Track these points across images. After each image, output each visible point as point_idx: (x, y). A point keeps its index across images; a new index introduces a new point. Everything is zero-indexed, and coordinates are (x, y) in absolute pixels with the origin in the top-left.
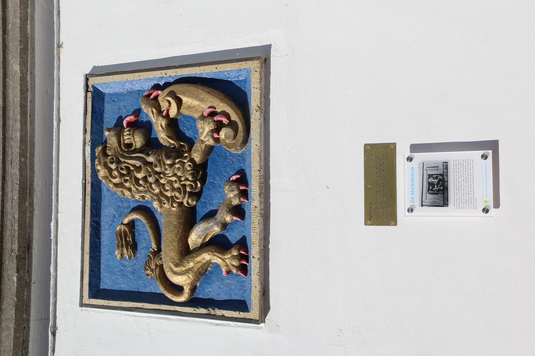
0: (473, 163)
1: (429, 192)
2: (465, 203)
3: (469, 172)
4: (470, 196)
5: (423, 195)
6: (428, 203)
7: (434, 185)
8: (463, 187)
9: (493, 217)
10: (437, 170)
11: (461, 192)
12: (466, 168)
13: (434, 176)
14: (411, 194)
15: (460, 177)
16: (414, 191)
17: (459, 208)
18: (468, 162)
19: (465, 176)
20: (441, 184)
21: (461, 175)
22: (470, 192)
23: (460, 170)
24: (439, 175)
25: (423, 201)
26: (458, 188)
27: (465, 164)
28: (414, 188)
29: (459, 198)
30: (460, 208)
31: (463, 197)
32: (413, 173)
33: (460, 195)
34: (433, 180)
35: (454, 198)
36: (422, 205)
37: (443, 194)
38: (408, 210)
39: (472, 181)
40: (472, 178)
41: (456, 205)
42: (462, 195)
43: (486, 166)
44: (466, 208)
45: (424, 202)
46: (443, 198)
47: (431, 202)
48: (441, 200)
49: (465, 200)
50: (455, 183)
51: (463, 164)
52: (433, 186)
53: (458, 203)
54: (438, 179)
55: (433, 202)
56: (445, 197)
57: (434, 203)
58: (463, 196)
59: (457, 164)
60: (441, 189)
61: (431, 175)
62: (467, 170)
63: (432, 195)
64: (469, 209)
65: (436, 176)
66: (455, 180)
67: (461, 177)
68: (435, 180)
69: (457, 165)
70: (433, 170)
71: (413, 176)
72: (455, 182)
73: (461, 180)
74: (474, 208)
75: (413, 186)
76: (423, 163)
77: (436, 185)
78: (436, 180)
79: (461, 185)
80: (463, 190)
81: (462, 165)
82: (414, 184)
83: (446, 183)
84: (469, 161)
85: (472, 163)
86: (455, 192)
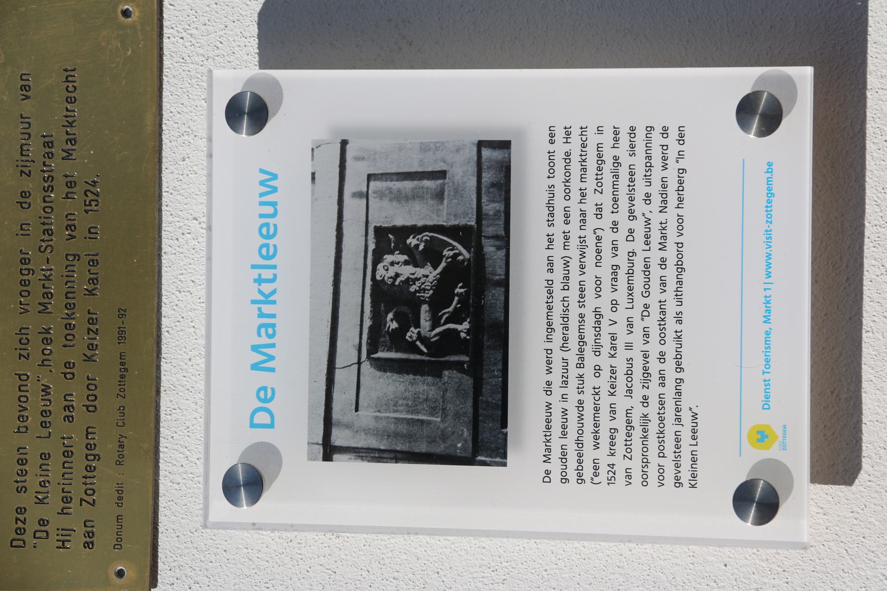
0: (680, 155)
1: (381, 355)
2: (621, 437)
3: (656, 219)
4: (654, 390)
5: (339, 375)
6: (367, 431)
7: (415, 303)
8: (613, 329)
9: (805, 547)
10: (439, 195)
12: (632, 188)
13: (412, 241)
14: (255, 367)
15: (591, 253)
16: (273, 346)
17: (580, 480)
18: (648, 148)
19: (624, 247)
20: (463, 299)
21: (599, 239)
22: (654, 367)
23: (592, 199)
24: (453, 231)
25: (336, 415)
26: (573, 334)
27: (625, 160)
28: (273, 326)
29: (581, 402)
30: (588, 473)
31: (605, 401)
32: (274, 215)
33: (590, 381)
34: (407, 271)
35: (549, 406)
36: (329, 451)
37: (476, 370)
39: (672, 285)
40: (672, 261)
41: (556, 454)
42: (603, 382)
43: (769, 181)
44: (629, 476)
45: (340, 424)
46: (470, 403)
47: (392, 427)
48: (457, 415)
50: (558, 294)
51: (616, 158)
52: (405, 309)
53: (570, 442)
54: (443, 265)
55: (403, 428)
56: (489, 396)
57: (409, 437)
58: (605, 389)
59: (575, 158)
60: (456, 332)
61: (394, 230)
62: (640, 207)
63: (396, 376)
64: (645, 483)
65: (430, 244)
66: (558, 276)
67: (599, 252)
68: (420, 272)
69: (575, 168)
70: (407, 198)
71: (268, 232)
72: (557, 287)
73: (598, 272)
74: (678, 483)
75: (267, 309)
76: (344, 143)
77: (425, 308)
78: (427, 270)
80: (606, 350)
81: (608, 167)
82: (274, 292)
83: (494, 295)
84: (657, 139)
85: (672, 154)
86: (557, 356)
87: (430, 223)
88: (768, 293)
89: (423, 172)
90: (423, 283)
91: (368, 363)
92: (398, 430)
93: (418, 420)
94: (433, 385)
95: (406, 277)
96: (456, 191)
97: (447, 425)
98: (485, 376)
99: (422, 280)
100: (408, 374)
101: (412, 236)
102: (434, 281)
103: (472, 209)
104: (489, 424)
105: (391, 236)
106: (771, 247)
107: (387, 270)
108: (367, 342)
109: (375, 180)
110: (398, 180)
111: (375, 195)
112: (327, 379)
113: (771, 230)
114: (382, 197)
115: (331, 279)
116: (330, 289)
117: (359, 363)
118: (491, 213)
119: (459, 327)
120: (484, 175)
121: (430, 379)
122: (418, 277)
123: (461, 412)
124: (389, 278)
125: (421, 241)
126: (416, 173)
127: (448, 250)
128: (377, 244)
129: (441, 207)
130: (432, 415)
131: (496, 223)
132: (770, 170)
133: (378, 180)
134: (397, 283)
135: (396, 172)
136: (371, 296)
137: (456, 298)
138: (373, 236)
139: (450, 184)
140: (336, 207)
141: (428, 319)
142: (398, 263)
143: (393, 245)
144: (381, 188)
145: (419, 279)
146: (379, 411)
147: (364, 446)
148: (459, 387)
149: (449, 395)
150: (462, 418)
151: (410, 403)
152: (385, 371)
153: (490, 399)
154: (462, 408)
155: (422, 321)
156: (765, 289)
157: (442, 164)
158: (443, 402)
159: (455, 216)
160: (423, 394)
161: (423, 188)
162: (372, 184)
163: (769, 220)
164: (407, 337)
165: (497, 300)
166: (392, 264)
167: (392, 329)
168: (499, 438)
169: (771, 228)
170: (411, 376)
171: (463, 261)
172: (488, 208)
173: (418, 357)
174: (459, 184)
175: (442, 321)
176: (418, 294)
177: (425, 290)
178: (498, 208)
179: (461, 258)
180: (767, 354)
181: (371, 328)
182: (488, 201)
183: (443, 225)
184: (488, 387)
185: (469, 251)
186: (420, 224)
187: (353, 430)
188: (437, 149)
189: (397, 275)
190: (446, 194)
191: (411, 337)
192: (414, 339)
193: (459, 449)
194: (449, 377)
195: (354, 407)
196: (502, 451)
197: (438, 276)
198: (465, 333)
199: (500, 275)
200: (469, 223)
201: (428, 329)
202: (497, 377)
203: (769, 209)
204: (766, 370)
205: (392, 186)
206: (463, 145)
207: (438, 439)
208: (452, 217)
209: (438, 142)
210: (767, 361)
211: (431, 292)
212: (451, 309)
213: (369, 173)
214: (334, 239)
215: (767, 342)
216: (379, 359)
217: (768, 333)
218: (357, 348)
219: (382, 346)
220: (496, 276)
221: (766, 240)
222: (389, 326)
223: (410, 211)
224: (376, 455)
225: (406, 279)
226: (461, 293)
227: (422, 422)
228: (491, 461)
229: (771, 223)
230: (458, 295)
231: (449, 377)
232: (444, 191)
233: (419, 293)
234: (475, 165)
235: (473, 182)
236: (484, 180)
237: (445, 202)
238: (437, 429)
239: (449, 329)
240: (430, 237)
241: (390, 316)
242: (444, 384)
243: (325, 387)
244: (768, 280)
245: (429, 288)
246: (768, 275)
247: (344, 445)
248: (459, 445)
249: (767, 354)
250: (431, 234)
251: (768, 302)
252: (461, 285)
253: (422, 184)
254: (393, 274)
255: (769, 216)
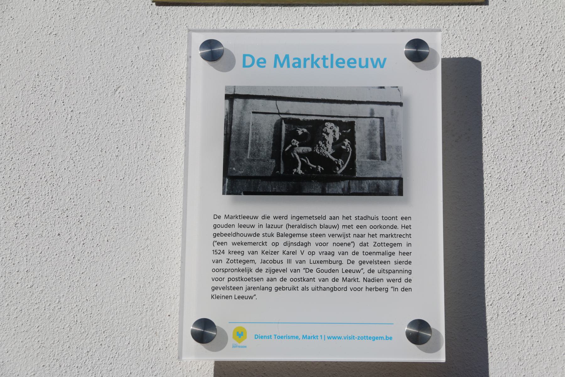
0: (395, 289)
1: (284, 125)
3: (360, 276)
5: (272, 103)
6: (242, 118)
7: (312, 143)
8: (299, 253)
9: (179, 358)
11: (281, 244)
12: (377, 262)
13: (347, 142)
14: (277, 57)
16: (288, 66)
17: (215, 235)
18: (399, 271)
19: (344, 259)
21: (349, 245)
22: (278, 275)
23: (371, 241)
25: (250, 101)
27: (392, 259)
28: (299, 66)
29: (258, 235)
30: (219, 239)
31: (259, 248)
32: (361, 66)
33: (270, 240)
34: (330, 139)
35: (256, 218)
36: (231, 97)
37: (275, 177)
38: (210, 44)
39: (323, 284)
40: (336, 284)
41: (230, 222)
44: (218, 262)
45: (245, 103)
46: (257, 174)
47: (244, 132)
48: (250, 167)
49: (247, 257)
50: (318, 222)
51: (393, 254)
52: (309, 138)
53: (236, 230)
54: (334, 159)
55: (243, 138)
57: (238, 141)
59: (393, 231)
60: (296, 167)
61: (353, 132)
62: (366, 267)
63: (272, 134)
64: (214, 270)
65: (345, 152)
66: (328, 222)
67: (341, 244)
68: (330, 146)
70: (370, 139)
71: (351, 63)
72: (322, 222)
73: (330, 244)
74: (214, 289)
75: (309, 63)
76: (401, 104)
77: (310, 149)
78: (331, 151)
79: (307, 244)
80: (287, 249)
81: (389, 249)
82: (318, 67)
83: (317, 187)
84: (405, 276)
85: (396, 284)
86: (283, 222)
87: (357, 152)
88: (319, 337)
89: (385, 148)
90: (323, 148)
91: (279, 119)
92: (242, 135)
93: (248, 146)
94: (267, 154)
95: (327, 139)
96: (375, 166)
97: (245, 162)
98: (272, 182)
99: (325, 148)
100: (273, 140)
101: (349, 142)
102: (325, 154)
103: (365, 175)
104: (246, 185)
105: (349, 130)
106: (345, 339)
107: (331, 128)
108: (291, 118)
109: (380, 121)
110: (380, 134)
111: (372, 121)
112: (270, 96)
113: (354, 339)
114: (371, 125)
115: (326, 98)
116: (320, 98)
117: (279, 114)
118: (363, 185)
119: (299, 168)
120: (384, 181)
121: (270, 152)
122: (327, 146)
123: (252, 169)
124: (326, 129)
125: (347, 147)
126: (385, 144)
127: (342, 162)
128: (345, 123)
129: (366, 157)
130: (251, 154)
131: (357, 188)
132: (387, 338)
133: (381, 123)
134: (323, 134)
135: (385, 133)
136: (316, 120)
137: (315, 167)
138: (349, 121)
139: (378, 163)
140: (365, 100)
141: (304, 151)
142: (334, 134)
143: (345, 131)
144: (376, 124)
145: (326, 146)
146: (253, 124)
147: (233, 117)
148: (266, 168)
149: (262, 163)
150: (249, 170)
151: (257, 142)
152: (275, 128)
153: (259, 185)
154: (255, 170)
155: (302, 148)
156: (321, 336)
157: (390, 158)
158: (258, 160)
159: (361, 166)
160: (262, 149)
161: (376, 148)
162: (378, 120)
163: (360, 338)
164: (293, 140)
165: (314, 189)
166: (334, 131)
167: (298, 132)
168: (238, 190)
169: (356, 339)
170: (272, 142)
171: (336, 170)
172: (366, 184)
173: (283, 146)
174: (378, 167)
175: (302, 159)
176: (317, 145)
177: (320, 149)
178: (365, 189)
179: (338, 169)
180: (286, 337)
181: (298, 120)
182: (369, 183)
183: (355, 158)
184: (266, 184)
185: (341, 173)
186: (356, 146)
187: (242, 111)
188: (398, 155)
189: (328, 134)
190: (373, 160)
191: (294, 142)
192: (293, 144)
193: (232, 169)
194: (271, 163)
195: (255, 111)
196: (231, 192)
197: (327, 157)
198: (296, 171)
199: (328, 190)
200: (357, 173)
201: (298, 151)
202: (272, 189)
203: (366, 338)
204: (276, 336)
205: (377, 131)
206: (400, 170)
207: (238, 157)
208: (360, 164)
209: (402, 156)
210: (281, 337)
211: (319, 153)
212: (309, 163)
213: (384, 118)
214: (347, 99)
215: (292, 337)
216: (281, 124)
217: (297, 337)
218: (287, 112)
219: (289, 126)
220: (328, 188)
221: (348, 336)
222: (300, 130)
223: (363, 141)
224: (228, 124)
225: (326, 139)
226: (318, 169)
227: (247, 148)
228: (225, 186)
229: (358, 339)
230: (317, 167)
231: (271, 163)
232: (374, 159)
233: (318, 146)
234: (389, 177)
235: (379, 175)
236: (381, 181)
237: (369, 160)
238: (243, 157)
239: (298, 162)
240: (349, 152)
241: (305, 130)
242: (268, 160)
243: (266, 95)
244: (326, 338)
245: (321, 151)
246: (329, 338)
247: (234, 106)
248: (234, 169)
249: (286, 337)
250: (351, 152)
251: (314, 338)
252: (323, 169)
253: (378, 147)
254: (328, 132)
255: (362, 338)
